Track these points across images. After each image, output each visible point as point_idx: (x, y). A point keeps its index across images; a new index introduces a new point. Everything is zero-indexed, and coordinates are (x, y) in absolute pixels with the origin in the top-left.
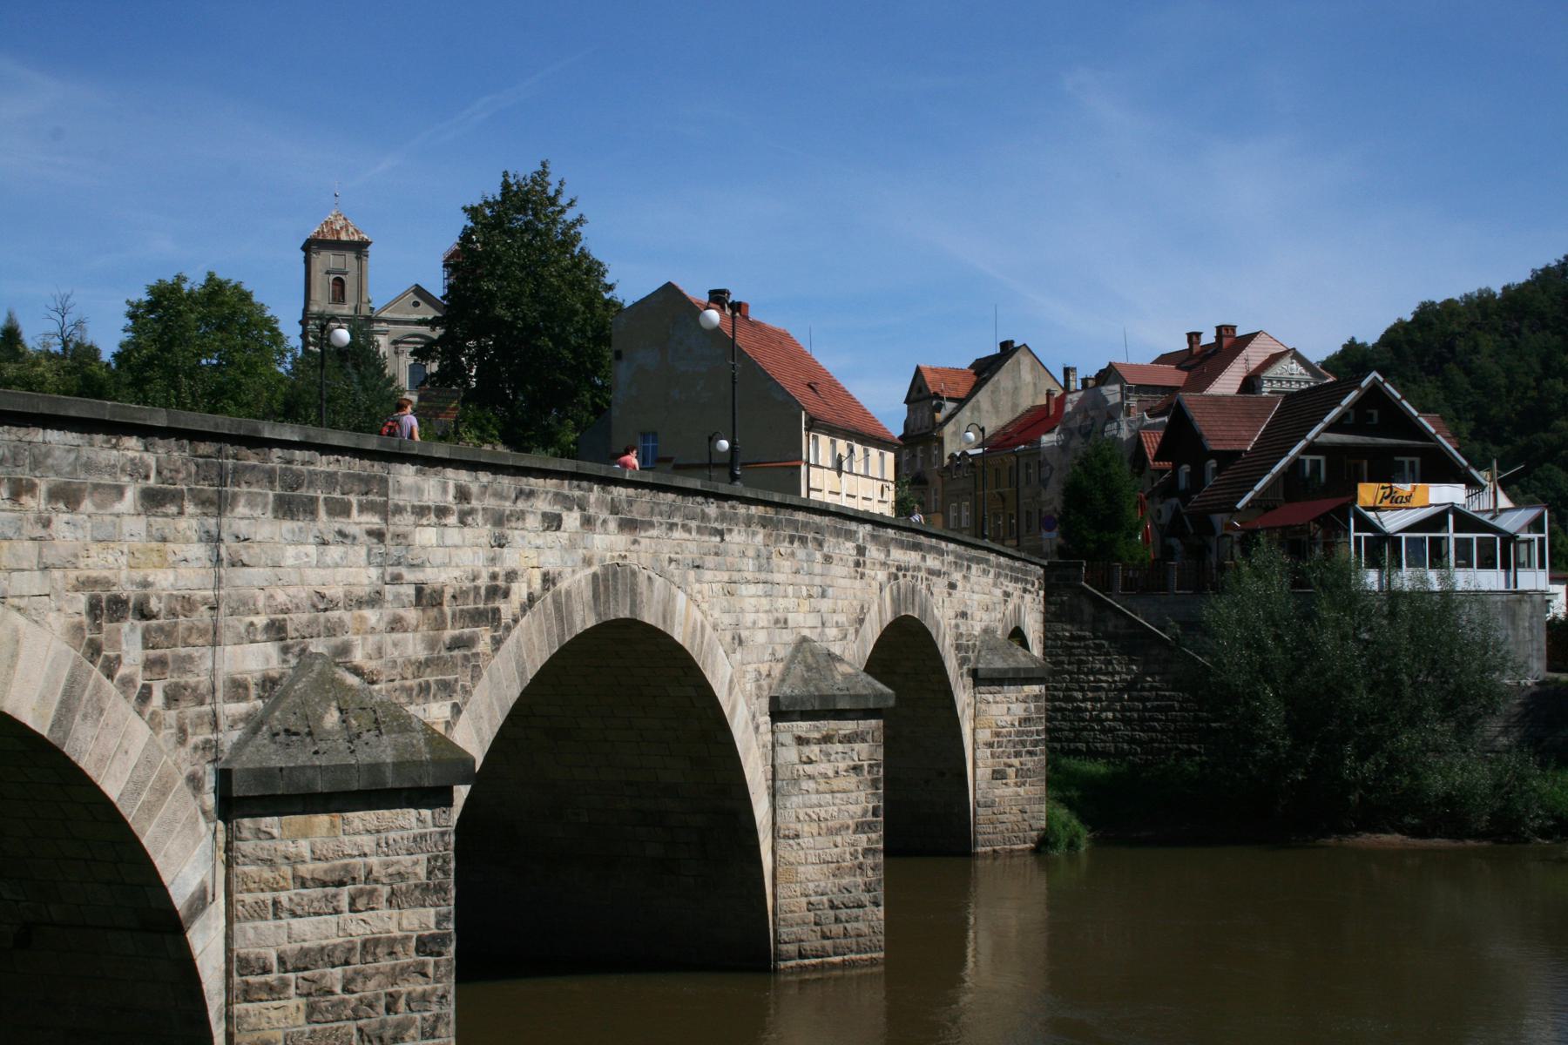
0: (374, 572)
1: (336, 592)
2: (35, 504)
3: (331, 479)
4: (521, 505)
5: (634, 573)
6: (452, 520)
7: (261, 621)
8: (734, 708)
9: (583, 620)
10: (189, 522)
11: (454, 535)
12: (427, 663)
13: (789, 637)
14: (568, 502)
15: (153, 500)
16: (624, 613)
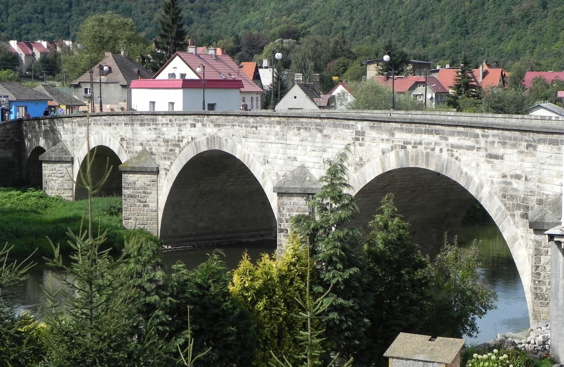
0: (155, 136)
1: (149, 139)
2: (115, 125)
3: (147, 119)
4: (185, 122)
5: (220, 138)
6: (169, 126)
7: (139, 143)
8: (265, 183)
9: (204, 148)
10: (129, 128)
11: (170, 128)
12: (165, 153)
13: (297, 164)
14: (198, 121)
15: (125, 124)
16: (217, 148)
